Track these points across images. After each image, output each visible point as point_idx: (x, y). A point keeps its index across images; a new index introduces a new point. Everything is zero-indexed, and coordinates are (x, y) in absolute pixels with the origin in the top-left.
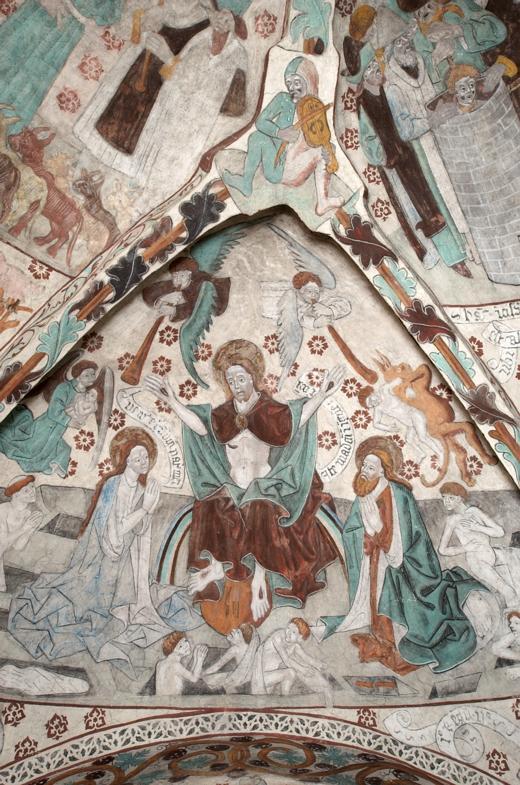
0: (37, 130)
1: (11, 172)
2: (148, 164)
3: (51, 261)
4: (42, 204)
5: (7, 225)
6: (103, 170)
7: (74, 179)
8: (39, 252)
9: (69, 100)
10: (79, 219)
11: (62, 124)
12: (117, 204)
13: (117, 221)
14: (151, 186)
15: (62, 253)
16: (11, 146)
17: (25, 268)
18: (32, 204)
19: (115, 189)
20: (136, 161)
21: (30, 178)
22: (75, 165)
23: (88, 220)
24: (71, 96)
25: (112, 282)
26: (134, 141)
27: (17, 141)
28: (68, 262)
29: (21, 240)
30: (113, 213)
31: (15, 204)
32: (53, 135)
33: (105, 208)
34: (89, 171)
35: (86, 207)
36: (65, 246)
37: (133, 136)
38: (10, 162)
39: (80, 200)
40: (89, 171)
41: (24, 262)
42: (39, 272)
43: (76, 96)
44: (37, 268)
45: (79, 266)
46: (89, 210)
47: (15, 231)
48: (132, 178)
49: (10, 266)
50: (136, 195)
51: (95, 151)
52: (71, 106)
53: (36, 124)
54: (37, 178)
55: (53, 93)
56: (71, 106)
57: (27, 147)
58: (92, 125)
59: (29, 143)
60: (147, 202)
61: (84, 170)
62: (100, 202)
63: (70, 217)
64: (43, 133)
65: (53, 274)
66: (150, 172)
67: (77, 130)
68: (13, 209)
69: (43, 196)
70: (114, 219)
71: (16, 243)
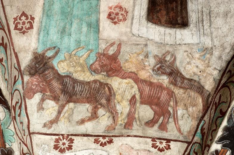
0: (107, 49)
1: (104, 88)
2: (206, 27)
3: (165, 135)
4: (138, 97)
5: (121, 124)
6: (171, 50)
7: (152, 67)
8: (154, 131)
9: (117, 14)
10: (171, 94)
11: (121, 34)
12: (195, 70)
13: (202, 84)
14: (217, 43)
15: (171, 125)
16: (94, 71)
17: (149, 147)
18: (130, 101)
19: (188, 60)
20: (194, 29)
21: (119, 84)
22: (147, 56)
23: (179, 92)
24: (117, 10)
25: (224, 146)
26: (184, 15)
27: (97, 66)
28: (179, 130)
29: (136, 129)
30: (196, 78)
31: (118, 107)
32: (120, 45)
33: (188, 77)
34: (160, 55)
35: (171, 83)
36: (171, 120)
37: (181, 10)
38: (100, 83)
39: (165, 80)
40: (160, 55)
41: (146, 143)
42: (161, 146)
43: (121, 8)
44: (158, 144)
45: (190, 131)
46: (175, 85)
47: (128, 125)
48: (198, 44)
49: (138, 150)
50: (208, 56)
51: (157, 39)
52: (121, 17)
53: (103, 46)
54: (125, 81)
55: (103, 17)
56: (121, 17)
57: (105, 65)
58: (144, 21)
59: (106, 61)
60: (220, 58)
61: (155, 57)
62: (181, 74)
63: (164, 96)
64: (112, 48)
65: (172, 144)
66: (211, 33)
67: (135, 31)
68: (119, 112)
69: (135, 90)
70: (199, 83)
71: (134, 133)
